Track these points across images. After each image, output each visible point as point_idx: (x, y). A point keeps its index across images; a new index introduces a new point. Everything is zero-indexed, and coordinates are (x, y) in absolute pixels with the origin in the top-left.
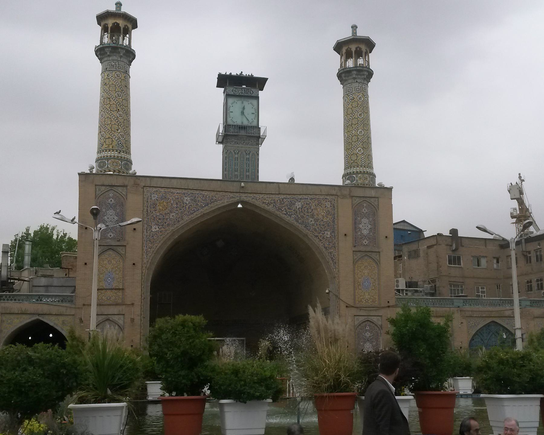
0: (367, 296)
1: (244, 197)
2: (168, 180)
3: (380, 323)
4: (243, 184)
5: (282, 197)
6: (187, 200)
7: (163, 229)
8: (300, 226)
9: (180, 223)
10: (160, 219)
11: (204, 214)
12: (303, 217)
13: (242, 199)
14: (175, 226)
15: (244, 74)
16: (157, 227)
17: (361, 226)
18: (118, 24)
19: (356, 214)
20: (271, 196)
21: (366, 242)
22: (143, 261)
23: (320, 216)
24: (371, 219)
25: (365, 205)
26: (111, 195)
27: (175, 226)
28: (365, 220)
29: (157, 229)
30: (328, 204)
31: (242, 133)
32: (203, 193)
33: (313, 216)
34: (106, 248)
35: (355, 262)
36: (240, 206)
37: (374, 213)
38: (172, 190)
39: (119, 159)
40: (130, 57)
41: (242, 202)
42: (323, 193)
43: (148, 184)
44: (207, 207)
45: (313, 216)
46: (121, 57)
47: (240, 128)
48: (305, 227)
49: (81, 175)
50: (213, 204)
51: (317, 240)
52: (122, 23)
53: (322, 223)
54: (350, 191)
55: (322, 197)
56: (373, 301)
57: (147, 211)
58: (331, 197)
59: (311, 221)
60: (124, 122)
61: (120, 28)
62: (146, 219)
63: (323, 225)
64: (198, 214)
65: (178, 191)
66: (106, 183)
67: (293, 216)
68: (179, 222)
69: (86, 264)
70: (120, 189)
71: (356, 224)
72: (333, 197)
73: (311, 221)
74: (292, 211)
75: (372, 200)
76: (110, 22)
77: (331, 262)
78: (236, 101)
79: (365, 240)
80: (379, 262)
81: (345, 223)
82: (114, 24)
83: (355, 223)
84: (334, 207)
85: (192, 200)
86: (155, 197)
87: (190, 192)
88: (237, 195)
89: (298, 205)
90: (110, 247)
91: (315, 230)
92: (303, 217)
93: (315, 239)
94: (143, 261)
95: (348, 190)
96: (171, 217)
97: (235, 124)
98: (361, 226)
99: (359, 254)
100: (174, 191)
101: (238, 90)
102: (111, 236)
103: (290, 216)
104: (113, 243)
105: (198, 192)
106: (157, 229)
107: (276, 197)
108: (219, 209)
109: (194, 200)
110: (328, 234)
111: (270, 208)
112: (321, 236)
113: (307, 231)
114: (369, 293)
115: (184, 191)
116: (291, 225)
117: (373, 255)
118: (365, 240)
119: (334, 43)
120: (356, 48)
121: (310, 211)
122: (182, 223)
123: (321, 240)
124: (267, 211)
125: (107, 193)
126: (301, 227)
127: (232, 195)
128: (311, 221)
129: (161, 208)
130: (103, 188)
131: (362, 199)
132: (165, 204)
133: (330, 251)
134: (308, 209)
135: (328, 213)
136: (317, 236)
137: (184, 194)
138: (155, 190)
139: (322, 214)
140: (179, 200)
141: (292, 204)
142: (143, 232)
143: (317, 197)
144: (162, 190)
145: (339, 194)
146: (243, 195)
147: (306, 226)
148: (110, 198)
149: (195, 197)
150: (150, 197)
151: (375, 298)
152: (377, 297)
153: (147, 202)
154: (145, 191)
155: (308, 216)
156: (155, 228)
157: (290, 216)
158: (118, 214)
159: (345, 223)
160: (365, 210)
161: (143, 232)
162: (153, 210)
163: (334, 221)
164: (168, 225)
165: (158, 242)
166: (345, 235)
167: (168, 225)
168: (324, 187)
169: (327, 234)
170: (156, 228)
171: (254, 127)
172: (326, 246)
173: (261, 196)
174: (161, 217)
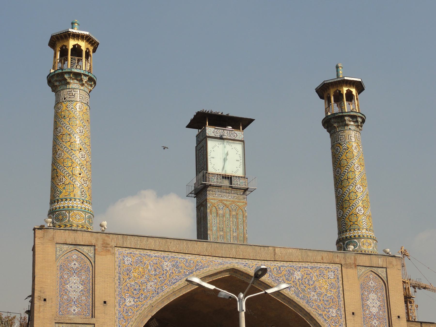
5: (279, 264)
6: (167, 266)
7: (139, 303)
9: (160, 295)
10: (135, 290)
14: (154, 299)
15: (224, 114)
16: (132, 300)
17: (368, 303)
18: (79, 47)
23: (323, 290)
24: (379, 294)
26: (75, 257)
27: (154, 299)
29: (133, 303)
30: (331, 275)
31: (226, 183)
32: (187, 257)
33: (315, 289)
38: (149, 252)
42: (325, 261)
43: (120, 244)
45: (315, 289)
47: (223, 177)
50: (198, 271)
53: (325, 298)
54: (355, 259)
55: (323, 266)
57: (120, 279)
61: (82, 51)
62: (118, 290)
63: (327, 301)
66: (69, 241)
68: (158, 294)
70: (85, 249)
71: (363, 299)
73: (313, 296)
74: (291, 282)
75: (380, 270)
76: (72, 43)
78: (218, 145)
79: (375, 321)
82: (74, 46)
83: (362, 299)
84: (338, 278)
85: (173, 266)
86: (128, 261)
87: (171, 255)
89: (298, 275)
91: (318, 306)
93: (320, 318)
95: (353, 257)
96: (149, 287)
97: (217, 172)
98: (368, 303)
100: (152, 253)
102: (74, 310)
105: (180, 256)
106: (133, 303)
109: (176, 266)
110: (333, 312)
112: (325, 315)
113: (310, 308)
115: (163, 254)
118: (375, 321)
119: (318, 83)
120: (347, 91)
121: (311, 282)
122: (162, 296)
126: (302, 303)
127: (220, 260)
129: (136, 275)
130: (65, 247)
132: (141, 270)
134: (308, 280)
135: (332, 286)
136: (320, 315)
137: (164, 257)
138: (128, 251)
139: (326, 287)
140: (158, 265)
141: (290, 273)
143: (319, 265)
144: (137, 252)
145: (343, 263)
147: (308, 302)
148: (73, 261)
149: (177, 262)
150: (122, 262)
153: (119, 266)
155: (309, 289)
158: (83, 281)
162: (126, 277)
164: (146, 297)
165: (133, 319)
166: (353, 313)
167: (146, 297)
168: (325, 254)
169: (333, 312)
170: (130, 302)
171: (239, 177)
174: (137, 288)
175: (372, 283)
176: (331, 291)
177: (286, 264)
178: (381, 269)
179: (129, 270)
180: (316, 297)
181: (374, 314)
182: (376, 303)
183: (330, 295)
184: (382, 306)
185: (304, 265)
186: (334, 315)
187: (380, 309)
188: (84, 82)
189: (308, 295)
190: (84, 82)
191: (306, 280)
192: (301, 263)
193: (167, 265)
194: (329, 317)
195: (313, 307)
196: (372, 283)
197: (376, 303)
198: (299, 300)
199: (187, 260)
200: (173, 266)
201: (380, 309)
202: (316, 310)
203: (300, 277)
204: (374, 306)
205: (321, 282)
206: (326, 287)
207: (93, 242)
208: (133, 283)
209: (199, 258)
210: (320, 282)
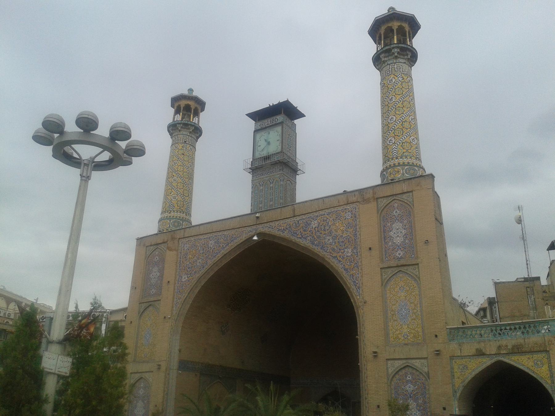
0: (405, 330)
1: (261, 229)
2: (198, 227)
3: (426, 369)
4: (258, 215)
5: (298, 218)
8: (316, 248)
10: (189, 268)
11: (225, 255)
12: (319, 237)
13: (258, 231)
19: (384, 218)
20: (287, 220)
21: (400, 253)
22: (172, 313)
23: (340, 232)
25: (396, 205)
28: (397, 225)
33: (330, 233)
34: (147, 304)
35: (384, 284)
36: (255, 238)
37: (410, 211)
39: (181, 220)
40: (189, 129)
41: (258, 235)
44: (227, 247)
46: (180, 131)
48: (321, 249)
49: (141, 241)
51: (336, 262)
52: (192, 104)
53: (341, 240)
55: (340, 209)
56: (414, 336)
58: (352, 206)
59: (329, 240)
60: (177, 186)
63: (343, 242)
64: (220, 256)
65: (206, 236)
67: (309, 238)
69: (131, 322)
70: (162, 246)
72: (354, 205)
73: (329, 240)
77: (353, 287)
79: (399, 252)
80: (419, 278)
81: (369, 232)
84: (355, 217)
88: (254, 227)
89: (314, 224)
90: (150, 303)
91: (333, 249)
92: (319, 237)
93: (334, 260)
94: (172, 313)
96: (198, 264)
99: (390, 272)
101: (267, 122)
103: (305, 238)
104: (152, 299)
107: (290, 221)
108: (238, 246)
110: (349, 252)
111: (286, 235)
113: (325, 253)
114: (408, 325)
116: (306, 248)
117: (410, 269)
118: (399, 252)
121: (327, 228)
123: (340, 261)
124: (284, 239)
125: (154, 252)
126: (317, 249)
128: (329, 240)
131: (390, 199)
132: (194, 251)
133: (352, 272)
137: (210, 238)
141: (307, 224)
142: (175, 283)
144: (192, 239)
146: (261, 226)
151: (418, 332)
152: (420, 330)
154: (180, 243)
155: (325, 234)
156: (185, 278)
157: (305, 238)
159: (369, 232)
160: (396, 213)
161: (175, 283)
163: (355, 235)
166: (370, 249)
167: (195, 272)
169: (348, 252)
172: (347, 267)
173: (277, 223)
175: (396, 212)
176: (347, 231)
177: (304, 217)
178: (406, 195)
179: (187, 254)
180: (331, 241)
181: (399, 244)
182: (401, 232)
183: (346, 235)
184: (408, 233)
185: (321, 212)
186: (350, 255)
187: (406, 237)
188: (179, 129)
189: (323, 241)
190: (179, 129)
191: (323, 227)
192: (317, 212)
193: (211, 243)
194: (343, 258)
195: (328, 251)
196: (396, 212)
197: (401, 232)
198: (314, 247)
199: (225, 235)
200: (215, 242)
201: (406, 237)
202: (331, 253)
203: (316, 225)
204: (398, 236)
205: (337, 225)
206: (341, 228)
207: (166, 240)
208: (188, 263)
209: (233, 232)
210: (337, 225)
